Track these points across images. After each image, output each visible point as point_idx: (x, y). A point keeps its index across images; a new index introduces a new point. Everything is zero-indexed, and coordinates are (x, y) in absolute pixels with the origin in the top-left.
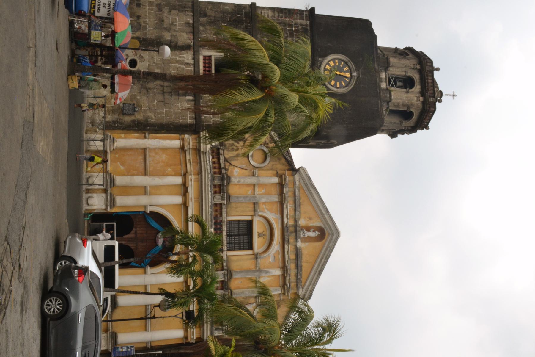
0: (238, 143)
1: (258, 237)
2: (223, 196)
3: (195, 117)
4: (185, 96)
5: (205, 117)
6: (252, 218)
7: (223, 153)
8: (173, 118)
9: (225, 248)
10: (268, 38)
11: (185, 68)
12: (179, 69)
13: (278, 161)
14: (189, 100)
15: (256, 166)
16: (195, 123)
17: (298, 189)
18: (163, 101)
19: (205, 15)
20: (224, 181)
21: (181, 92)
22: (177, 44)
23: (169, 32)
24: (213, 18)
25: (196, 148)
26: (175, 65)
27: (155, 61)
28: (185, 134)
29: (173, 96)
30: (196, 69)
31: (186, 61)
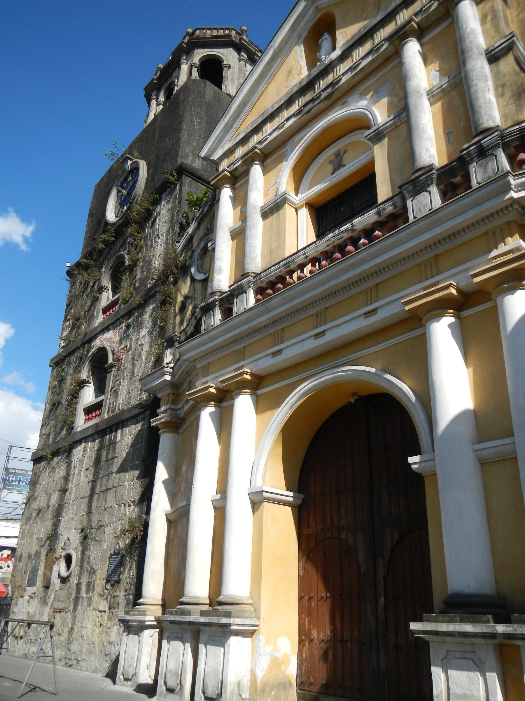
1: (344, 166)
2: (236, 292)
4: (116, 443)
6: (301, 207)
8: (137, 462)
9: (346, 230)
11: (88, 454)
12: (87, 467)
14: (122, 435)
17: (236, 139)
20: (210, 304)
24: (53, 421)
25: (171, 395)
26: (82, 475)
27: (72, 516)
31: (82, 453)
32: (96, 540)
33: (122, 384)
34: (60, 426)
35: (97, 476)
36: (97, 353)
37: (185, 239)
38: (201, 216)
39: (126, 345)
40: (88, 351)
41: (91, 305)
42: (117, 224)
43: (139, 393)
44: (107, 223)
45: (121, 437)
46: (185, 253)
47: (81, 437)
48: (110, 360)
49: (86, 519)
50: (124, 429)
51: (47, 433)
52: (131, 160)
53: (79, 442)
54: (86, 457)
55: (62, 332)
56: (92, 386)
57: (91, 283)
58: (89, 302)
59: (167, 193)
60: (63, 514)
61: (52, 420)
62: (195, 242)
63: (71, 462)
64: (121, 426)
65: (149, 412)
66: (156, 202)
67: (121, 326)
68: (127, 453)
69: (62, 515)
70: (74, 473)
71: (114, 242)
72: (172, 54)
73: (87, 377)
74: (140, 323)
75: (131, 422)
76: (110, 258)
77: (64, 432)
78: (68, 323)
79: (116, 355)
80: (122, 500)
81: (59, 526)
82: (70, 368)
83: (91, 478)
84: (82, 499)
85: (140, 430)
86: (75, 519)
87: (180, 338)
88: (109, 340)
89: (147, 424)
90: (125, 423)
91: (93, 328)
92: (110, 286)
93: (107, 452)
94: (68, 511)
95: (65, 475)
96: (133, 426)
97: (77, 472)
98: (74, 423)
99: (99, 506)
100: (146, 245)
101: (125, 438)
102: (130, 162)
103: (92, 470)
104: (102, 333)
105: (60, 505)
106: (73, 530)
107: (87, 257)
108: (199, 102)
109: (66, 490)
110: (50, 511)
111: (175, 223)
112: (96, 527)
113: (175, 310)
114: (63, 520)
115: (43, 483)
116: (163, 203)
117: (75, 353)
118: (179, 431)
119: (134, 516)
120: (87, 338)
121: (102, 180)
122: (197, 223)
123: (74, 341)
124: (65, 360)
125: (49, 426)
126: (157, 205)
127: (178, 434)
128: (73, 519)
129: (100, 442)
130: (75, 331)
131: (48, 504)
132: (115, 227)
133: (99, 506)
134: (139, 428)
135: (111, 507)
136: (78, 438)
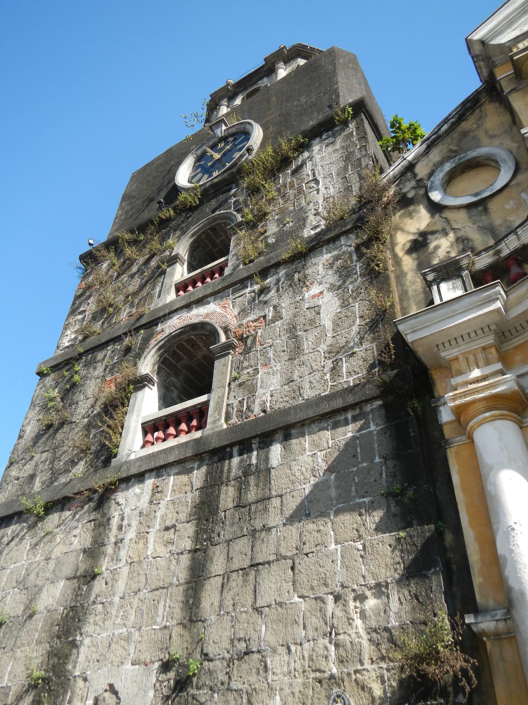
0: (437, 247)
3: (352, 407)
5: (349, 373)
7: (486, 250)
10: (125, 310)
11: (169, 498)
12: (168, 523)
13: (471, 134)
15: (513, 168)
16: (379, 403)
18: (290, 562)
19: (32, 477)
21: (251, 496)
22: (85, 551)
23: (40, 590)
24: (45, 455)
25: (493, 350)
28: (440, 427)
29: (271, 524)
30: (172, 458)
31: (146, 498)
32: (229, 689)
33: (262, 371)
34: (65, 458)
35: (210, 539)
36: (180, 334)
37: (399, 166)
38: (434, 136)
39: (263, 314)
40: (146, 341)
41: (142, 287)
42: (208, 184)
43: (328, 376)
44: (176, 190)
45: (283, 457)
46: (397, 185)
47: (143, 469)
48: (223, 339)
49: (181, 636)
50: (294, 441)
51: (26, 475)
52: (226, 125)
53: (133, 480)
54: (161, 506)
55: (66, 328)
56: (155, 388)
57: (141, 260)
58: (137, 282)
59: (324, 137)
60: (88, 628)
61: (42, 453)
62: (421, 170)
63: (109, 519)
64: (279, 436)
65: (379, 403)
66: (302, 147)
67: (241, 294)
68: (316, 486)
69: (83, 631)
70: (122, 540)
71: (197, 207)
72: (265, 59)
73: (152, 372)
74: (299, 280)
75: (314, 427)
76: (188, 228)
77: (80, 468)
78: (80, 317)
79: (235, 333)
80: (326, 585)
81: (73, 657)
82: (95, 368)
83: (188, 544)
84: (157, 592)
85: (354, 438)
86: (136, 636)
87: (473, 263)
88: (207, 315)
89: (377, 425)
90: (293, 431)
91: (160, 305)
92: (186, 258)
93: (240, 490)
94: (104, 620)
95: (88, 544)
96: (327, 434)
97: (131, 534)
98: (118, 447)
99: (228, 603)
100: (285, 195)
101: (305, 458)
102: (224, 128)
103: (190, 529)
104: (185, 310)
105: (72, 608)
106: (128, 666)
107: (134, 230)
108: (353, 67)
109: (94, 577)
110: (39, 622)
111: (359, 160)
112: (227, 656)
113: (395, 256)
114: (87, 641)
115: (12, 566)
116: (316, 148)
117: (107, 346)
118: (524, 420)
119: (394, 623)
120: (143, 321)
121: (148, 165)
122: (424, 146)
123: (99, 334)
124: (81, 358)
125: (33, 463)
126: (303, 152)
127: (521, 428)
128: (128, 639)
129: (208, 473)
130: (100, 323)
131: (27, 607)
132: (202, 188)
133: (228, 603)
134: (350, 435)
135: (280, 604)
136: (134, 471)
